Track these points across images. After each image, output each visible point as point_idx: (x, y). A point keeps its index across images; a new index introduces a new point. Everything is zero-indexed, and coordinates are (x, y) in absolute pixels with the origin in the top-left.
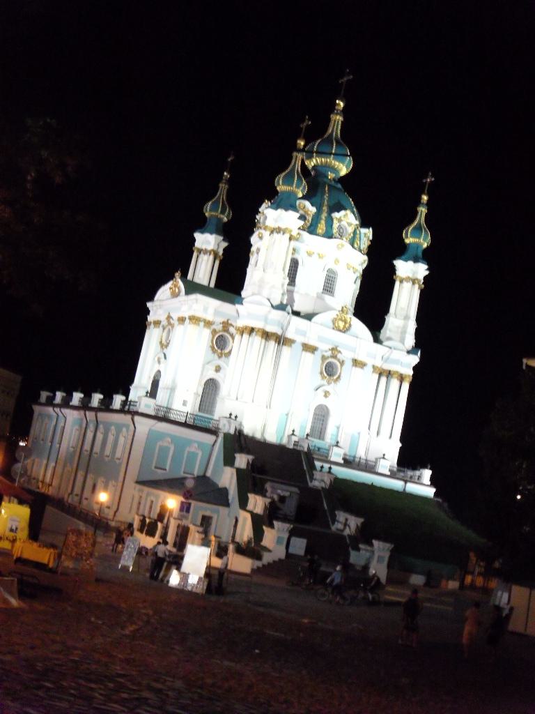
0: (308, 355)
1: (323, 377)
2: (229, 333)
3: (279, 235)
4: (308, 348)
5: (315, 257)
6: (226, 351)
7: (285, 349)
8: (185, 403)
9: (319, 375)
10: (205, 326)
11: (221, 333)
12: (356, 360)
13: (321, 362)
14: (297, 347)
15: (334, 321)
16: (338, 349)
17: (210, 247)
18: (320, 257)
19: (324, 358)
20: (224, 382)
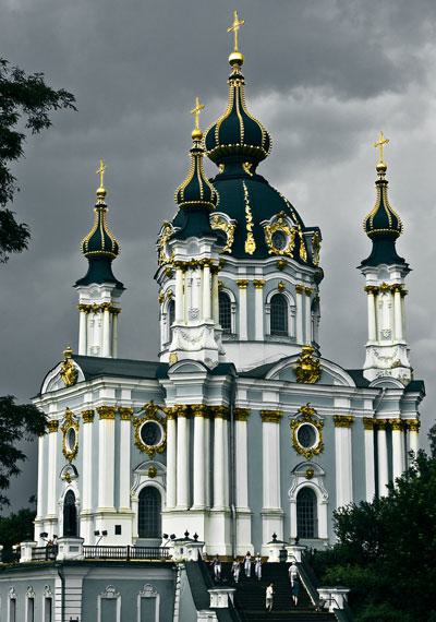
0: (270, 431)
2: (157, 419)
8: (118, 530)
14: (256, 418)
17: (99, 302)
18: (257, 284)
20: (165, 488)
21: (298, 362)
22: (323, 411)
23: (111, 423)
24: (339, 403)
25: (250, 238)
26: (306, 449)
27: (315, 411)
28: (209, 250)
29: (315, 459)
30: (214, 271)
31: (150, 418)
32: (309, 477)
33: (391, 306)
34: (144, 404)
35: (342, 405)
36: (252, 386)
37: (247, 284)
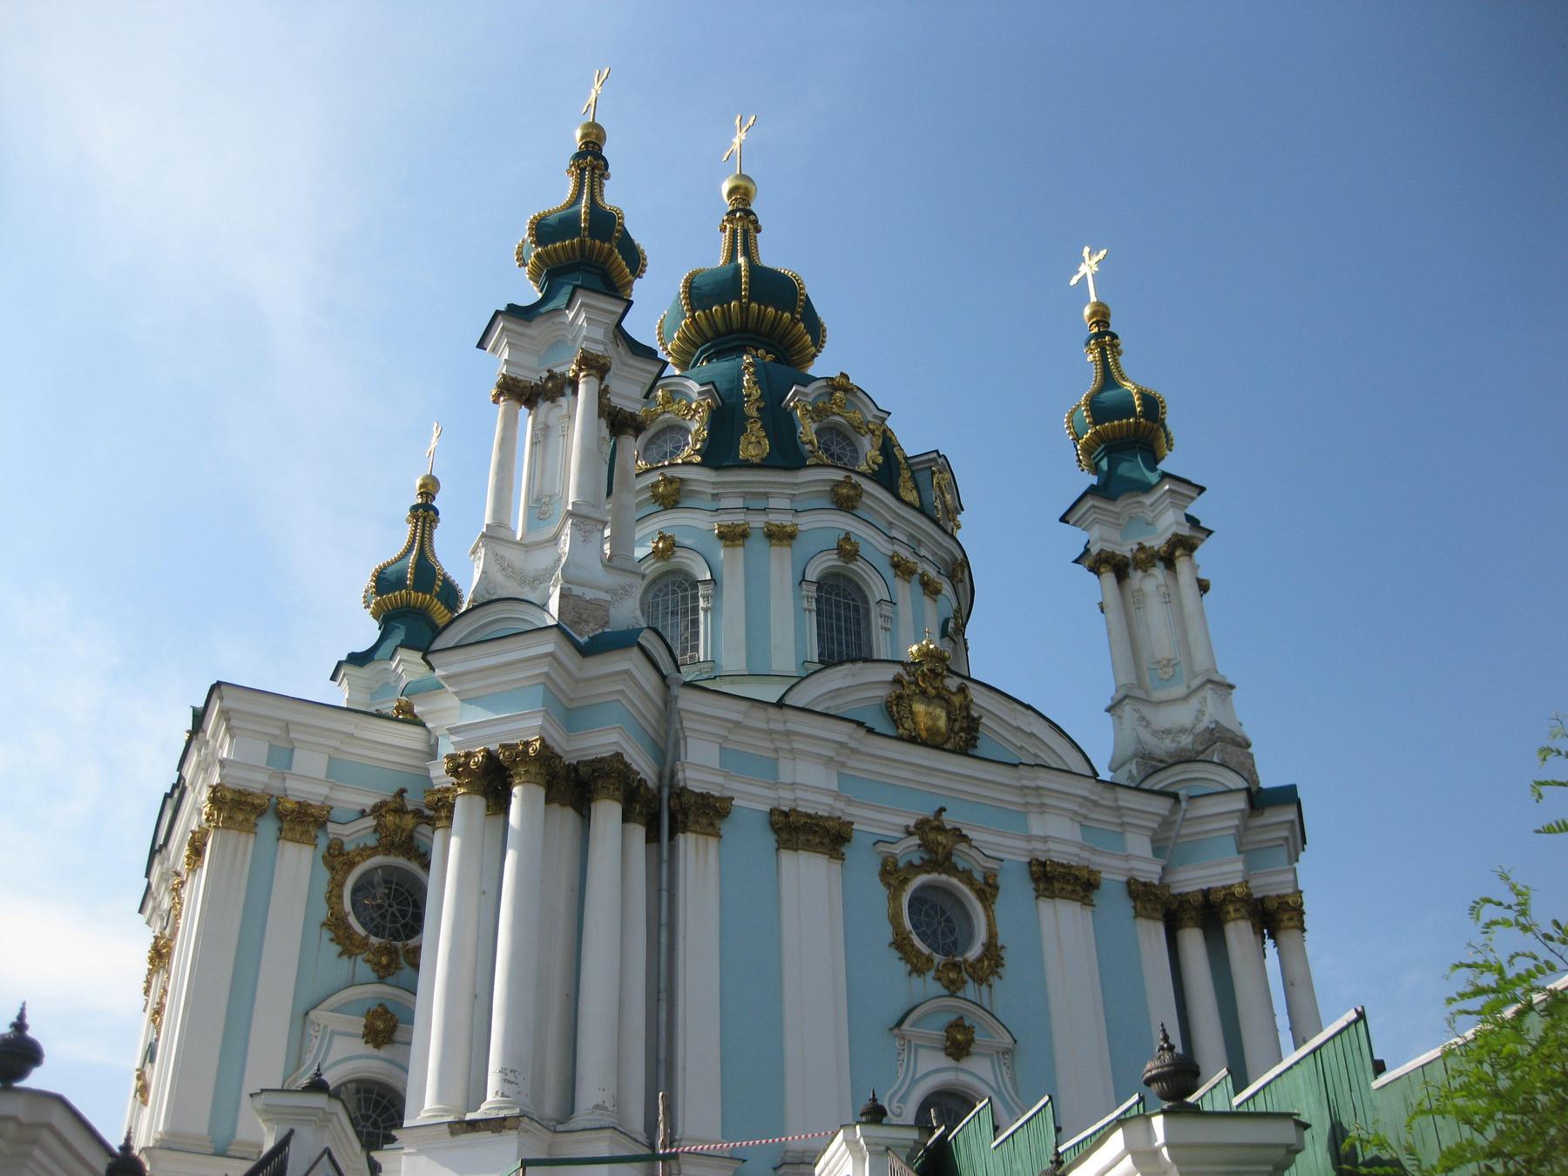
0: (807, 873)
1: (918, 966)
3: (563, 401)
4: (797, 830)
5: (757, 543)
6: (412, 943)
7: (688, 844)
9: (896, 954)
10: (281, 835)
11: (379, 860)
12: (1044, 864)
13: (882, 892)
14: (748, 833)
15: (895, 708)
16: (949, 820)
19: (893, 874)
21: (897, 681)
22: (999, 844)
23: (243, 844)
24: (1037, 826)
25: (755, 429)
26: (938, 958)
27: (965, 838)
28: (599, 333)
29: (970, 989)
30: (618, 423)
31: (387, 847)
32: (958, 1045)
33: (1170, 598)
34: (369, 801)
35: (1060, 837)
36: (737, 724)
37: (744, 535)
